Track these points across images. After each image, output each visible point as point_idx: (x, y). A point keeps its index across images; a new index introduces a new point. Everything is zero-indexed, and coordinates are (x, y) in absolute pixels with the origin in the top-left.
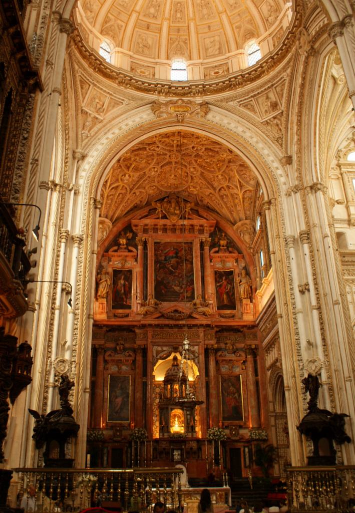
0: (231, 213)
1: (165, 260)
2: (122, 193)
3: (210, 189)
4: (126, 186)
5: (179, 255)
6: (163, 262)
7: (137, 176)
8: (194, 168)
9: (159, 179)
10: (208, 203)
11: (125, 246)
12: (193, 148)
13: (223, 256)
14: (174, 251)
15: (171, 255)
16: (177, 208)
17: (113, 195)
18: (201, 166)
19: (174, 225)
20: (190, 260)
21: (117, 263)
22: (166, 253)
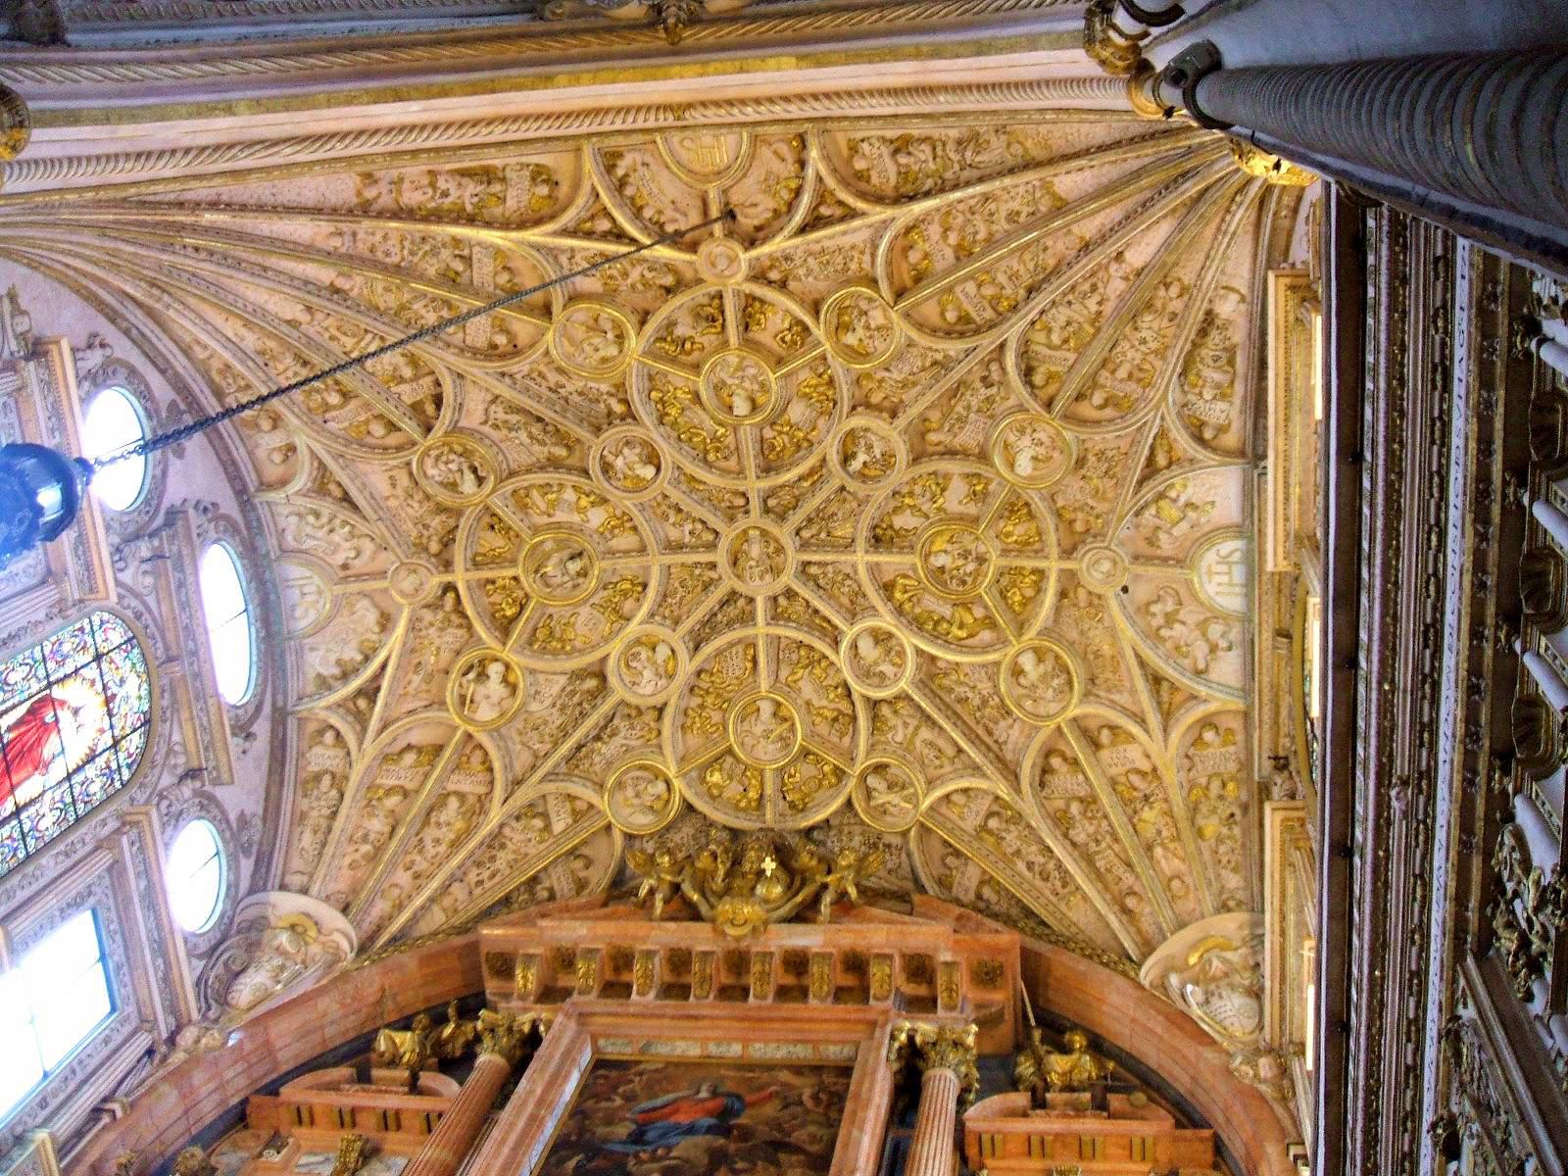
0: (1126, 911)
1: (638, 1138)
2: (462, 796)
3: (984, 776)
4: (482, 738)
5: (743, 1120)
6: (618, 1148)
7: (555, 690)
8: (881, 638)
9: (694, 740)
10: (987, 880)
11: (406, 1074)
12: (847, 458)
13: (1057, 1136)
14: (710, 1105)
15: (683, 1119)
16: (769, 865)
17: (405, 794)
18: (917, 624)
19: (738, 962)
20: (814, 1148)
21: (320, 1158)
22: (654, 1109)
